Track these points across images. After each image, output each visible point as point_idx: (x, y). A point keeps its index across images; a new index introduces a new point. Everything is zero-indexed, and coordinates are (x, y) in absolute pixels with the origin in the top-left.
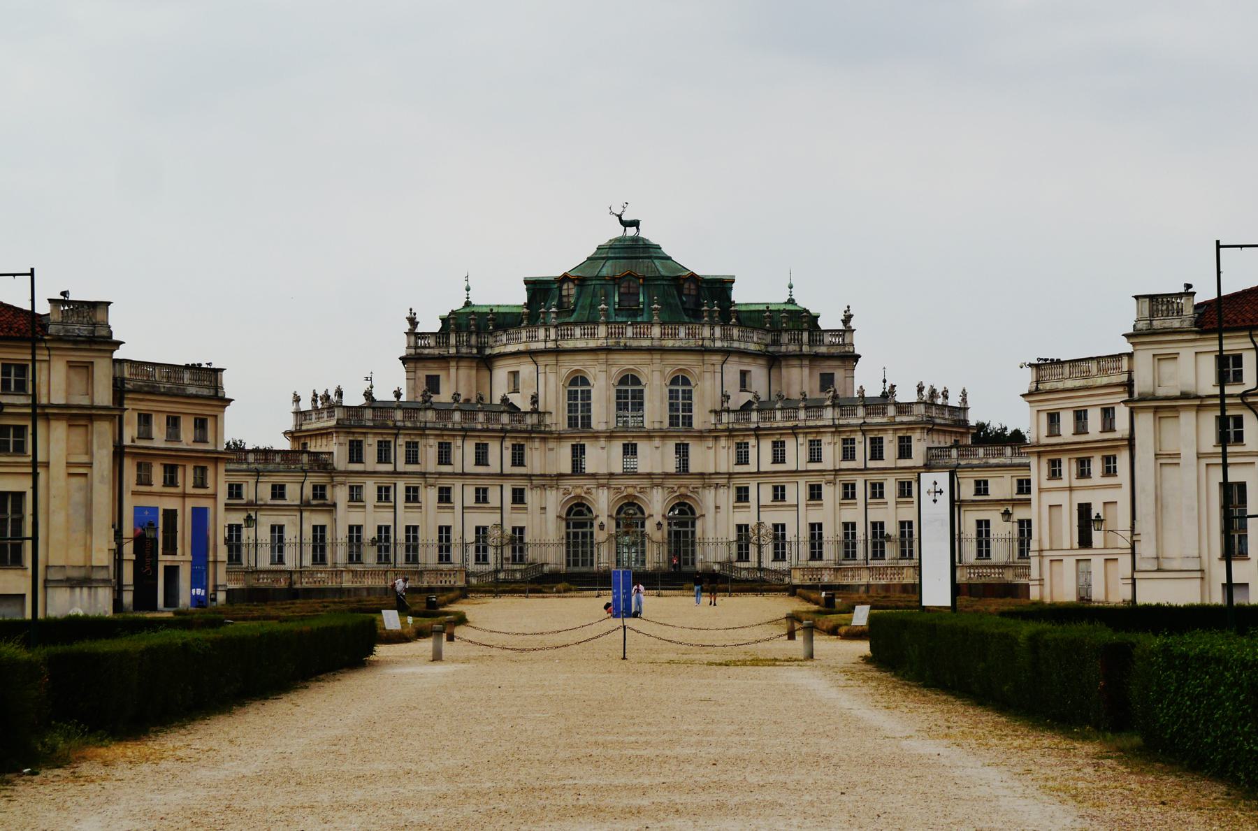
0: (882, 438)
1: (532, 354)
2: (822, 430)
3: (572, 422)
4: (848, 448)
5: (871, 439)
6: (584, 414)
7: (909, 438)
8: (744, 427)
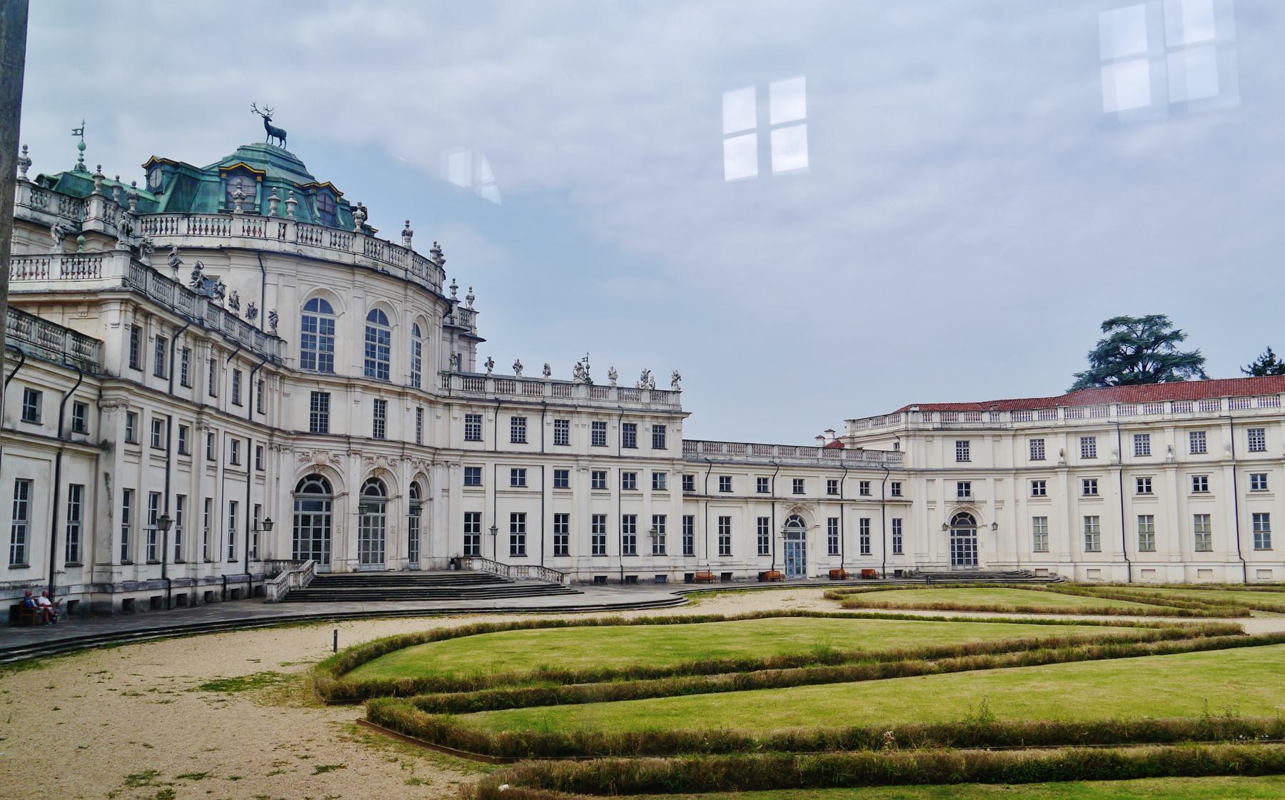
1: (260, 254)
2: (579, 410)
3: (307, 359)
4: (597, 432)
5: (624, 424)
7: (663, 428)
8: (477, 397)
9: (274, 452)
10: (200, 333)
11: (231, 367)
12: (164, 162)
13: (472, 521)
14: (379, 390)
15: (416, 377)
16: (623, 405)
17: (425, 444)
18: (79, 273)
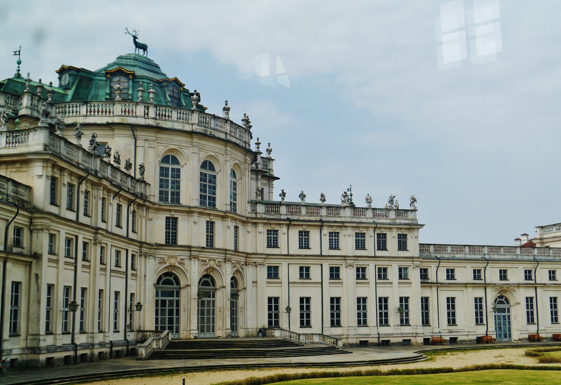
0: (385, 234)
2: (346, 224)
3: (163, 196)
4: (359, 240)
5: (378, 234)
6: (173, 190)
8: (274, 217)
9: (143, 259)
10: (95, 180)
11: (115, 202)
12: (71, 68)
13: (273, 302)
14: (209, 215)
15: (233, 205)
16: (376, 221)
17: (240, 251)
18: (16, 143)
